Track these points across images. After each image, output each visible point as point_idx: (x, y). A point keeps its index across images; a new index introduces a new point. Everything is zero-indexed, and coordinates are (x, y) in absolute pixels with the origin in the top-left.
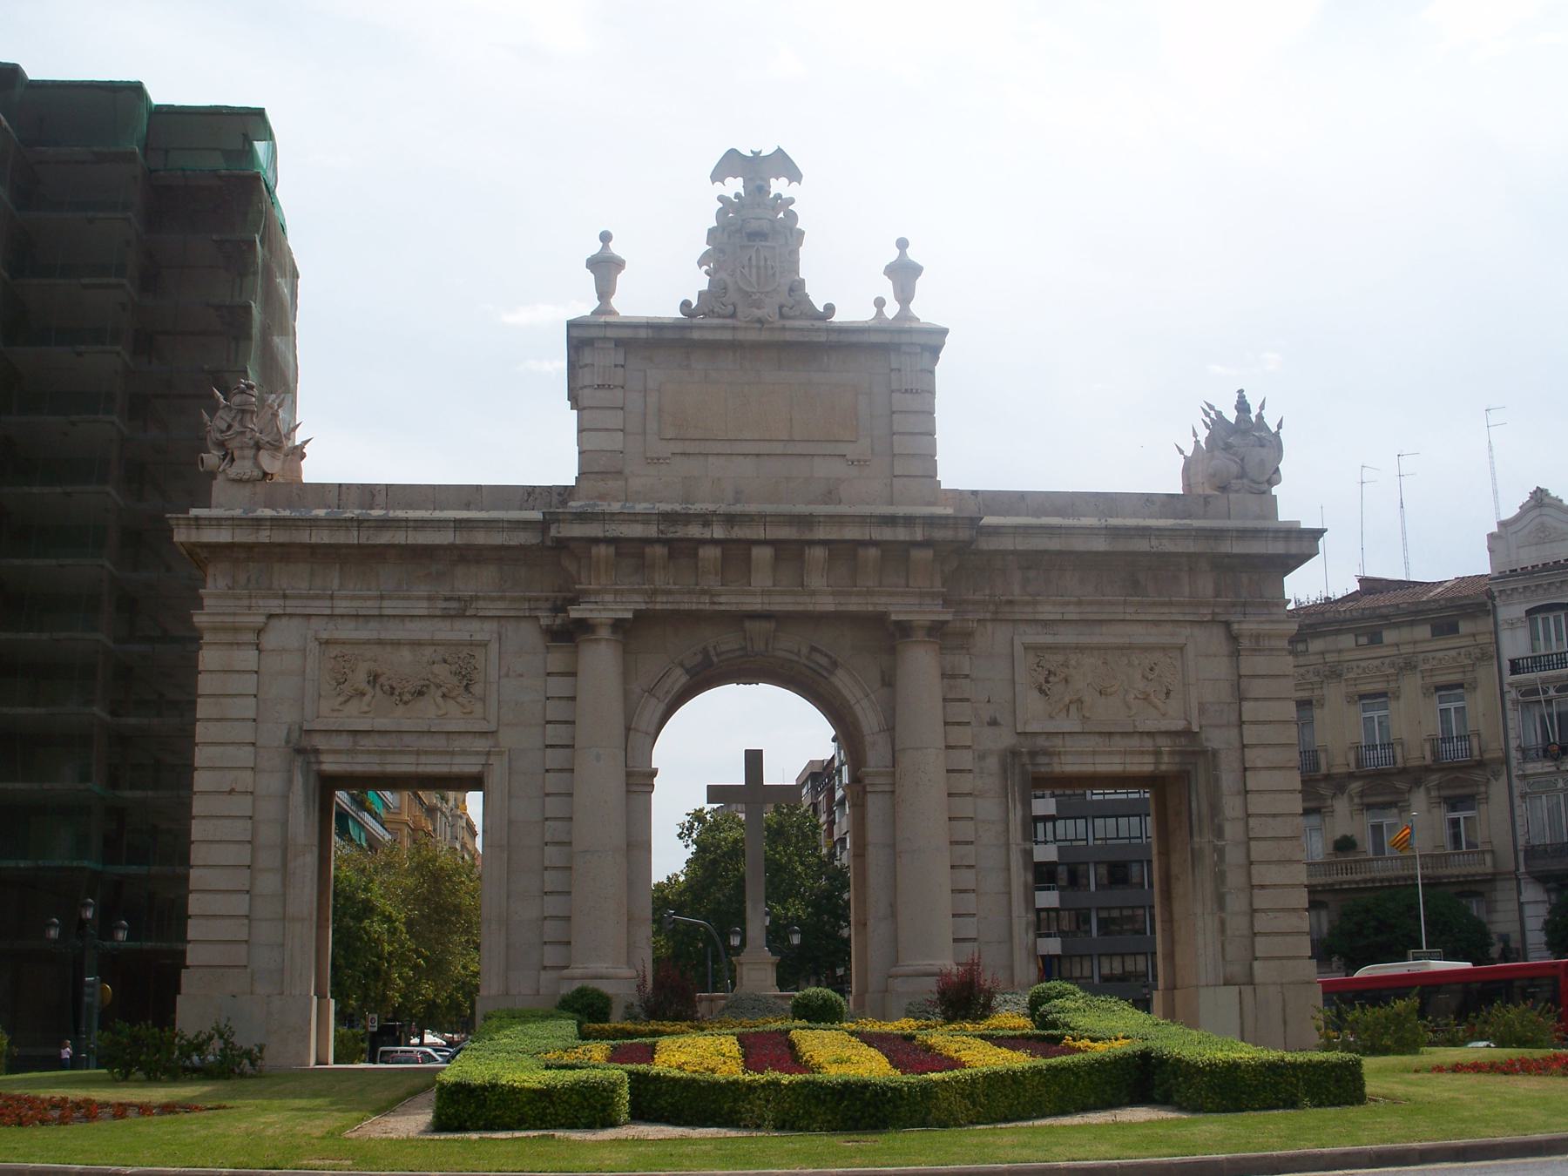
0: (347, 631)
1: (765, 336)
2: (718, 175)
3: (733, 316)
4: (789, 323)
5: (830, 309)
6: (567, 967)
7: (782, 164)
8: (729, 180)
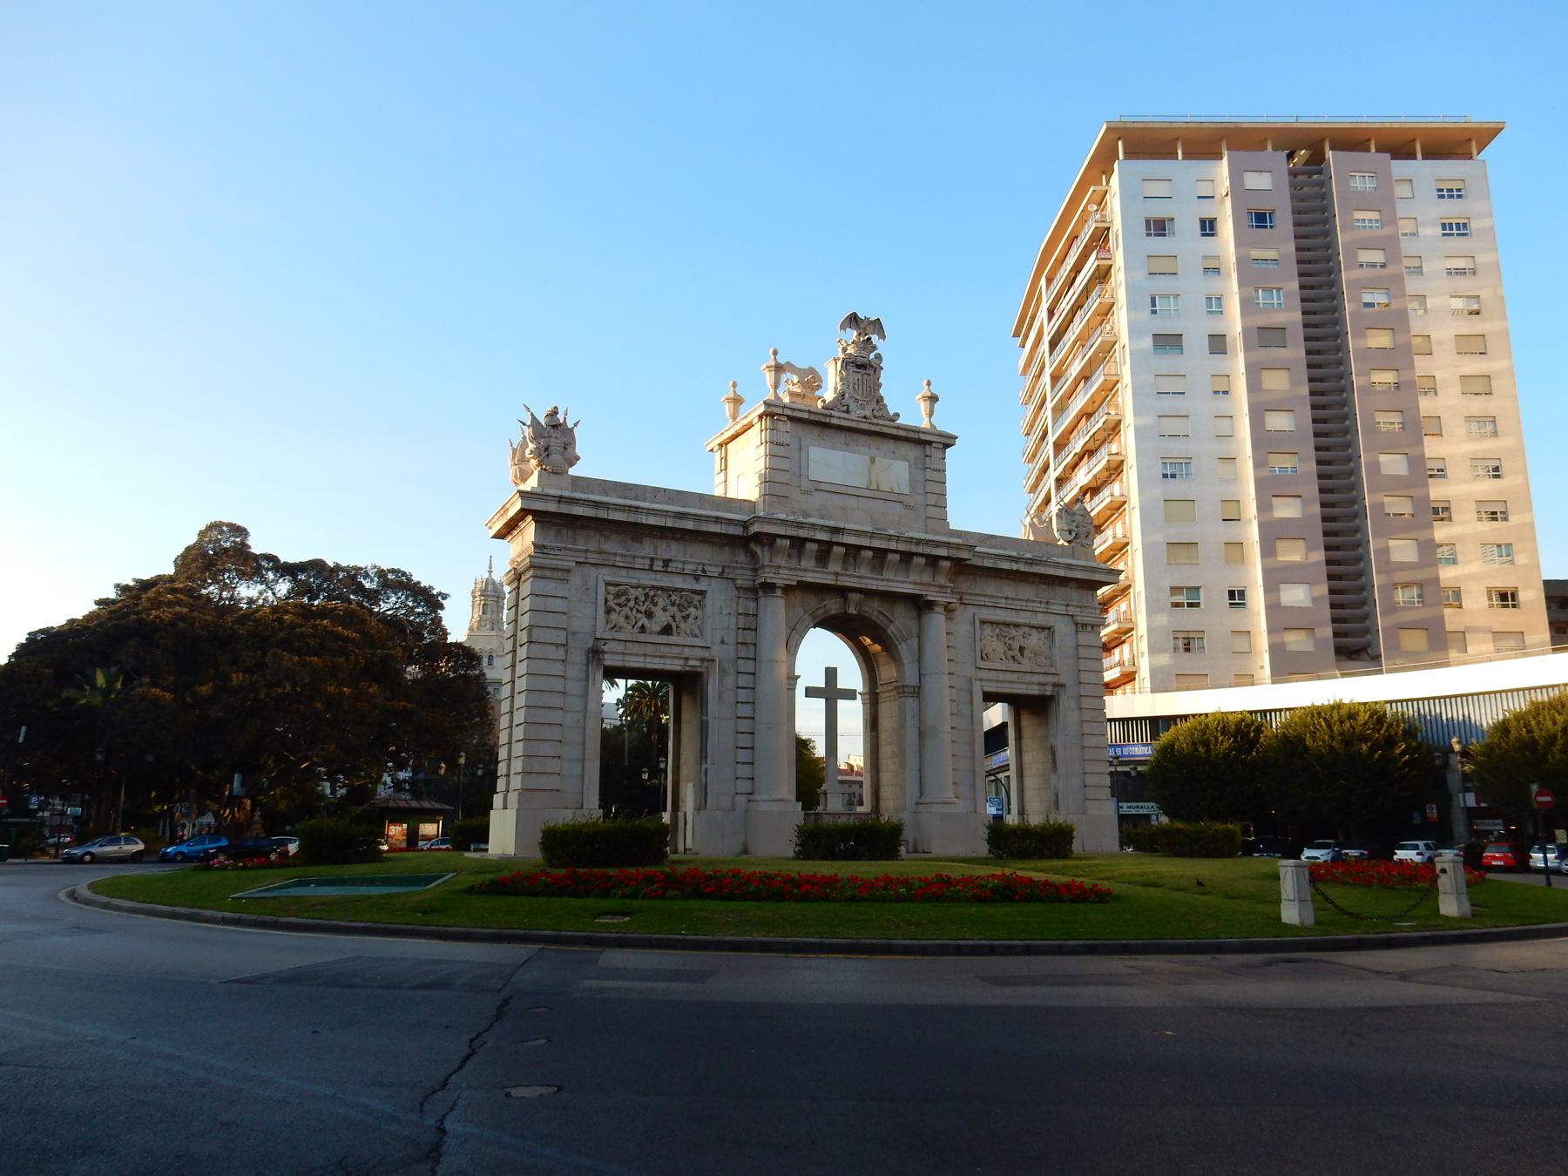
0: (622, 577)
1: (864, 426)
2: (843, 327)
3: (847, 412)
4: (875, 421)
5: (897, 415)
6: (751, 794)
7: (877, 325)
8: (848, 330)
